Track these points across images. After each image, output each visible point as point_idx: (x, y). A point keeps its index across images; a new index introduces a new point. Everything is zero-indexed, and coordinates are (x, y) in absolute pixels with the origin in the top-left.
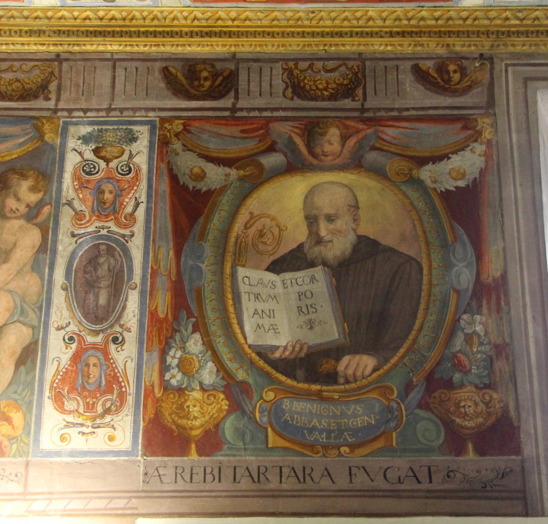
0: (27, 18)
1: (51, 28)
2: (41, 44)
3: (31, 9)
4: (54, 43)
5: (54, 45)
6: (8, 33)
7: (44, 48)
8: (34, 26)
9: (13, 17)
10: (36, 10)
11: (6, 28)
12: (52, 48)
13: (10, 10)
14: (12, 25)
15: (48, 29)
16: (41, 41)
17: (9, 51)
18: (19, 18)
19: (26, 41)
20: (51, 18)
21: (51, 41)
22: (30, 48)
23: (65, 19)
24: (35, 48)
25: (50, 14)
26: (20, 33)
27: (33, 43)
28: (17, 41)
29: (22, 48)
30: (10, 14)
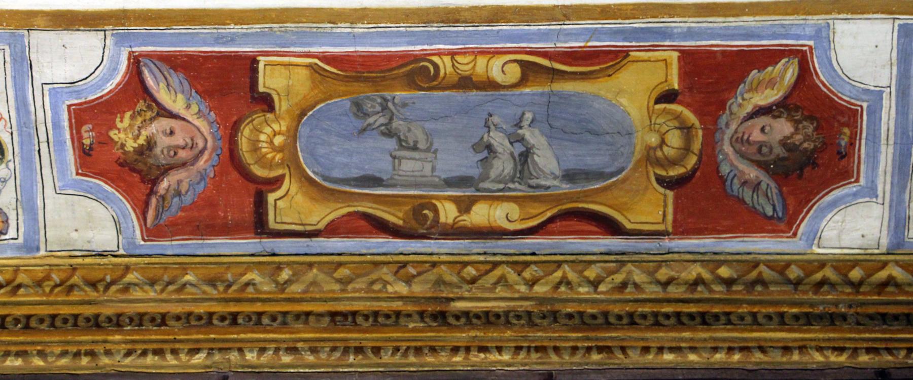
0: (797, 283)
1: (859, 310)
2: (834, 349)
3: (810, 262)
4: (871, 345)
5: (869, 350)
6: (749, 319)
7: (843, 358)
8: (812, 305)
9: (760, 281)
10: (822, 264)
11: (744, 309)
12: (864, 358)
13: (756, 264)
14: (760, 303)
15: (852, 311)
16: (834, 340)
17: (750, 367)
18: (776, 283)
19: (795, 340)
20: (861, 283)
21: (864, 340)
22: (806, 358)
23: (897, 285)
24: (818, 357)
25: (856, 274)
26: (782, 321)
27: (813, 344)
28: (771, 340)
29: (784, 359)
30: (754, 274)
